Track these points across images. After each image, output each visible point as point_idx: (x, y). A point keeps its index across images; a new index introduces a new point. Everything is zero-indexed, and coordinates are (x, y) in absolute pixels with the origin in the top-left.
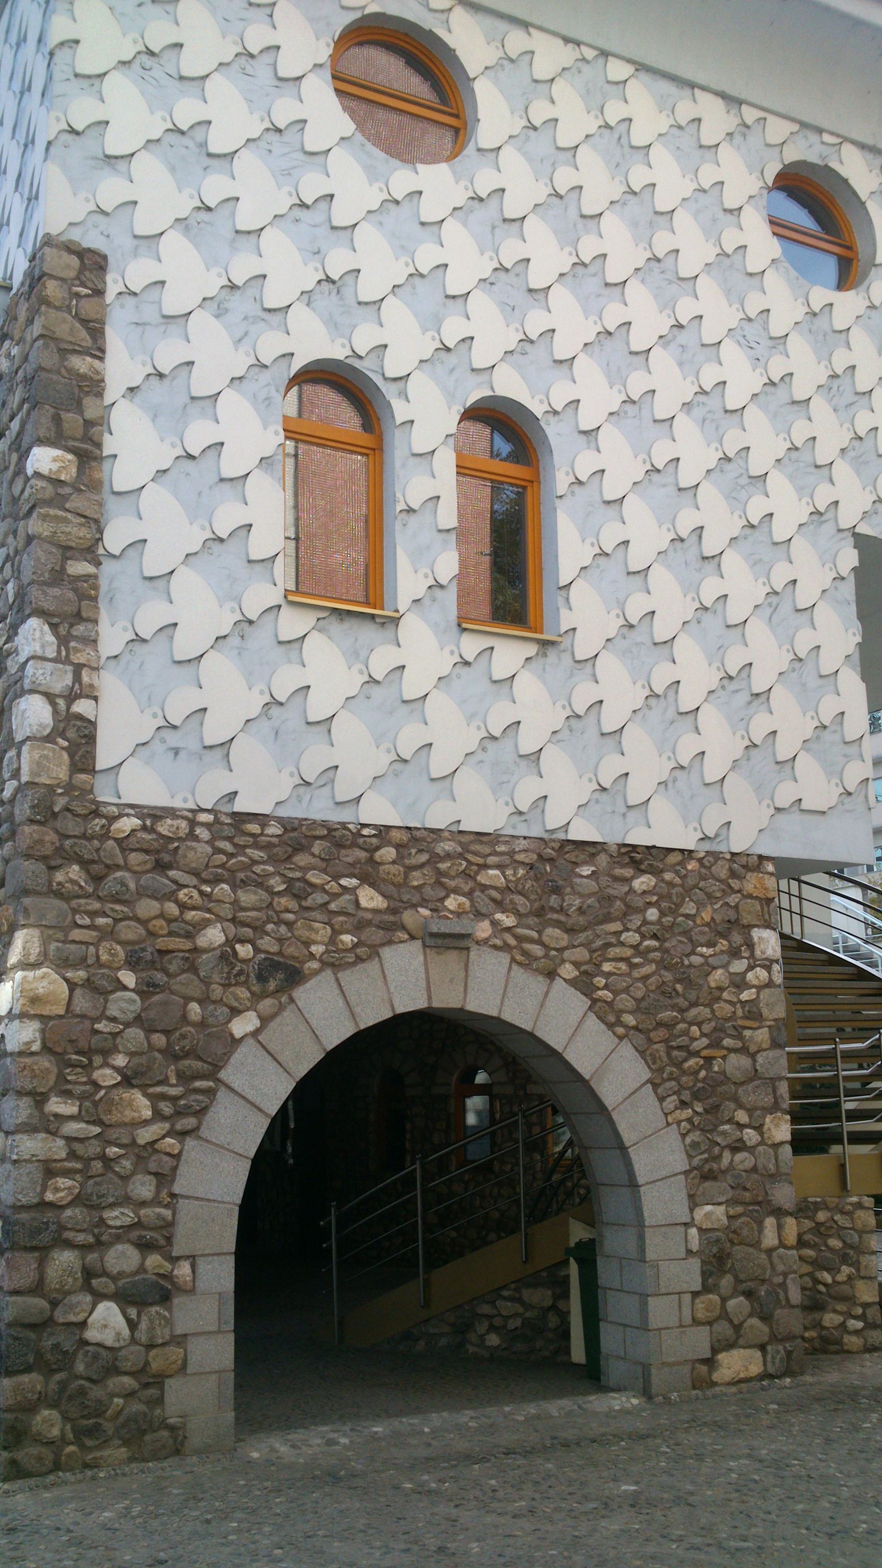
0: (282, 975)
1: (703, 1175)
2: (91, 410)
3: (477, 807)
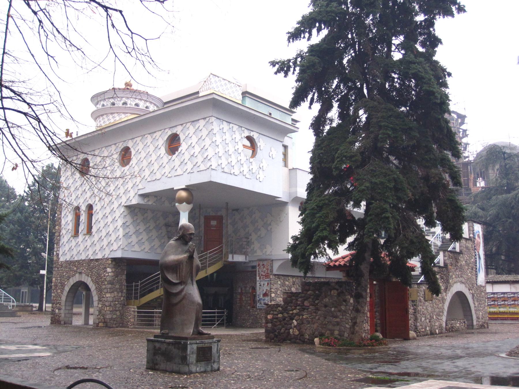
0: (69, 278)
1: (100, 300)
2: (60, 221)
3: (83, 257)
